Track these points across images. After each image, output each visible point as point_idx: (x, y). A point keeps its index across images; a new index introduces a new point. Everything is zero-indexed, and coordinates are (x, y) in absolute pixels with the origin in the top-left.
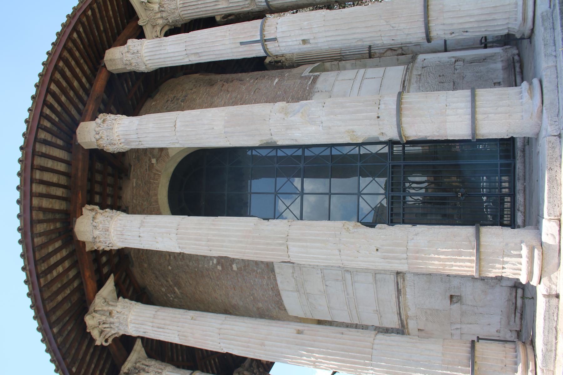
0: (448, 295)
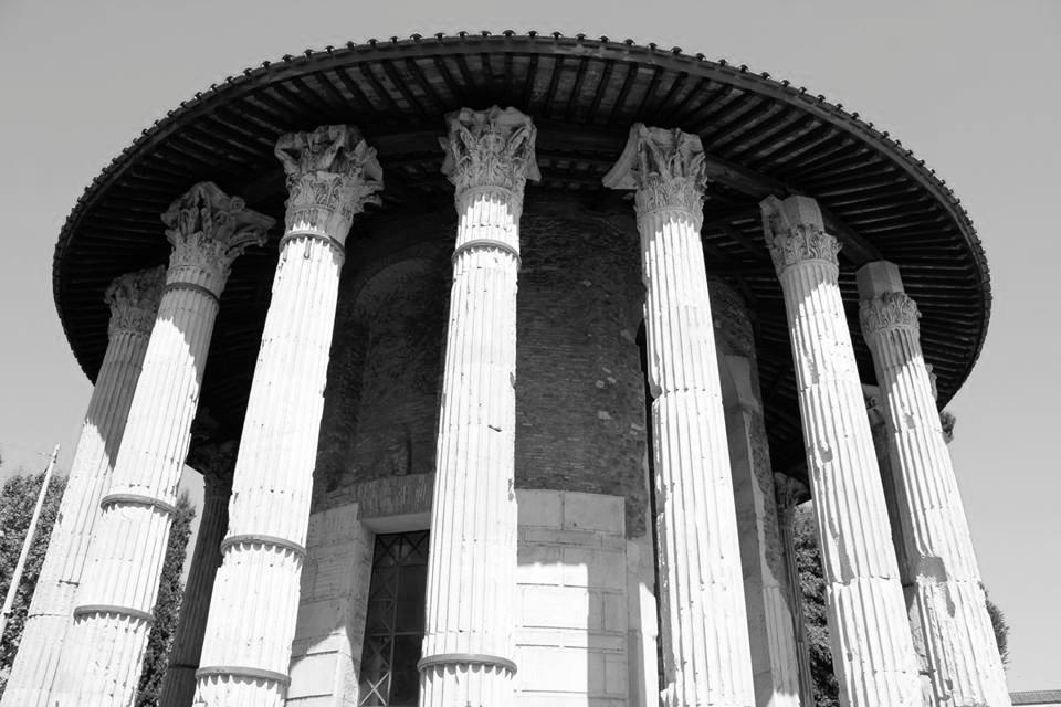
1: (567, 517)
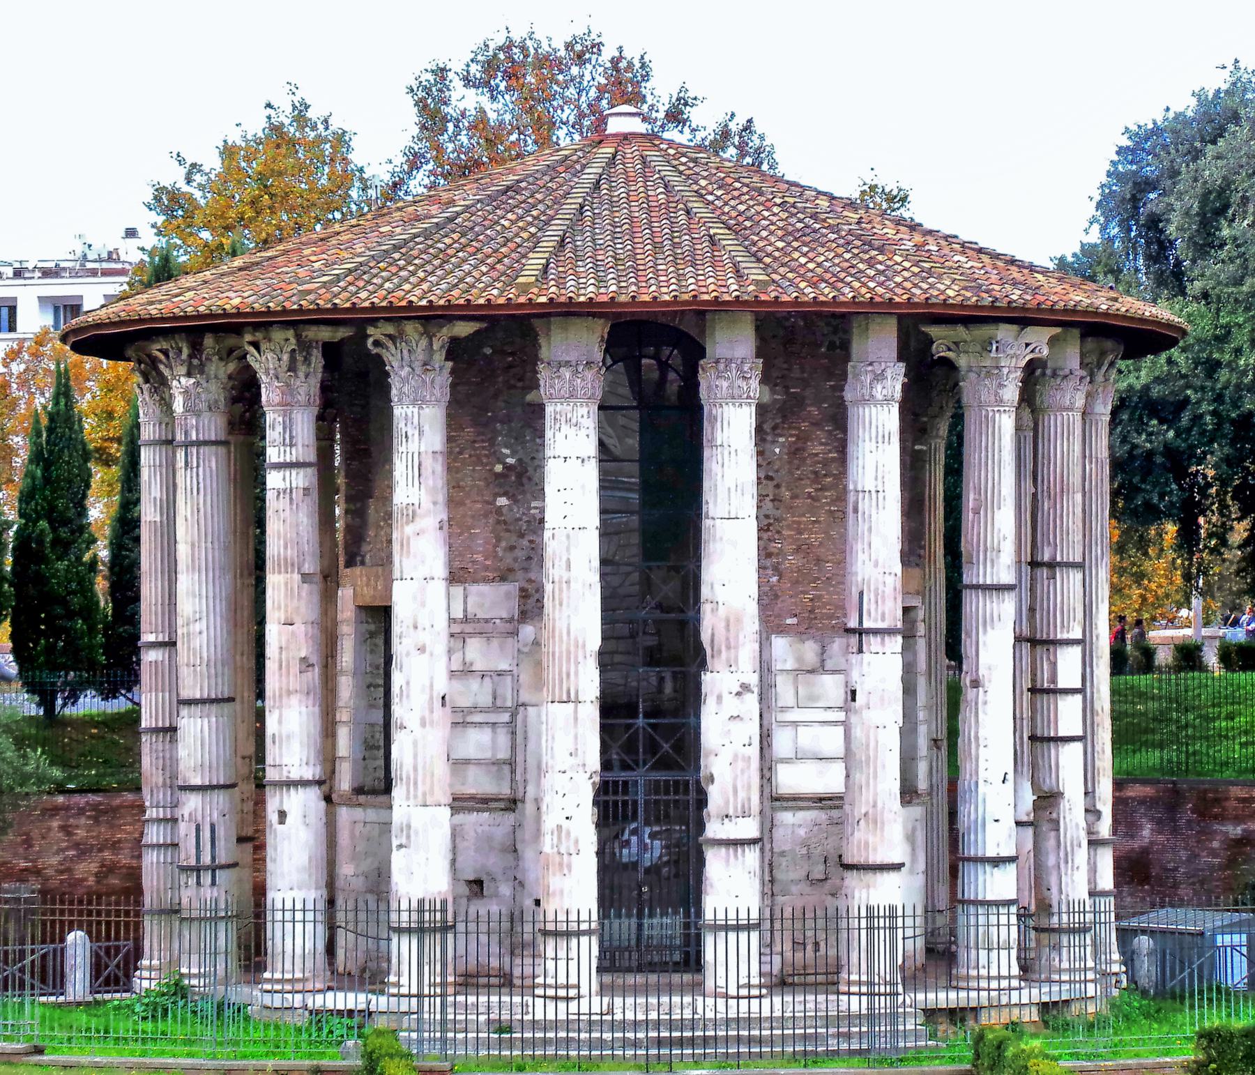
0: (484, 878)
1: (469, 609)
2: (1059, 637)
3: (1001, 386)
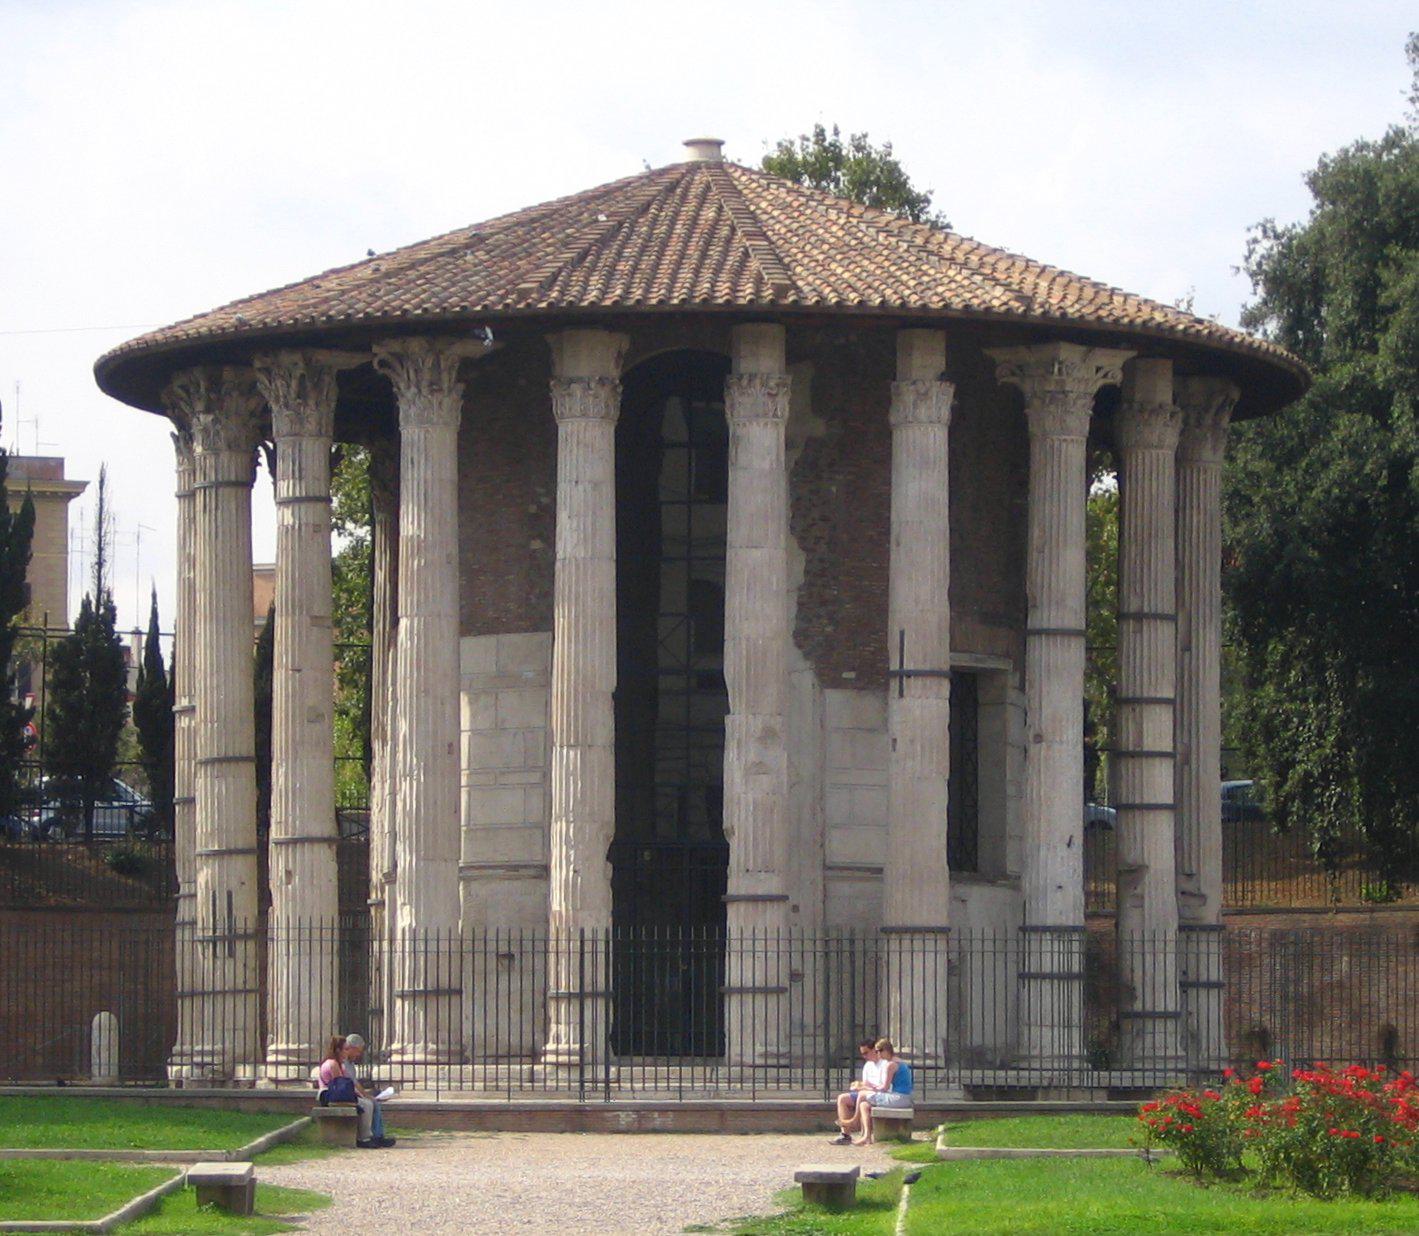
2: (1145, 695)
3: (1067, 412)
